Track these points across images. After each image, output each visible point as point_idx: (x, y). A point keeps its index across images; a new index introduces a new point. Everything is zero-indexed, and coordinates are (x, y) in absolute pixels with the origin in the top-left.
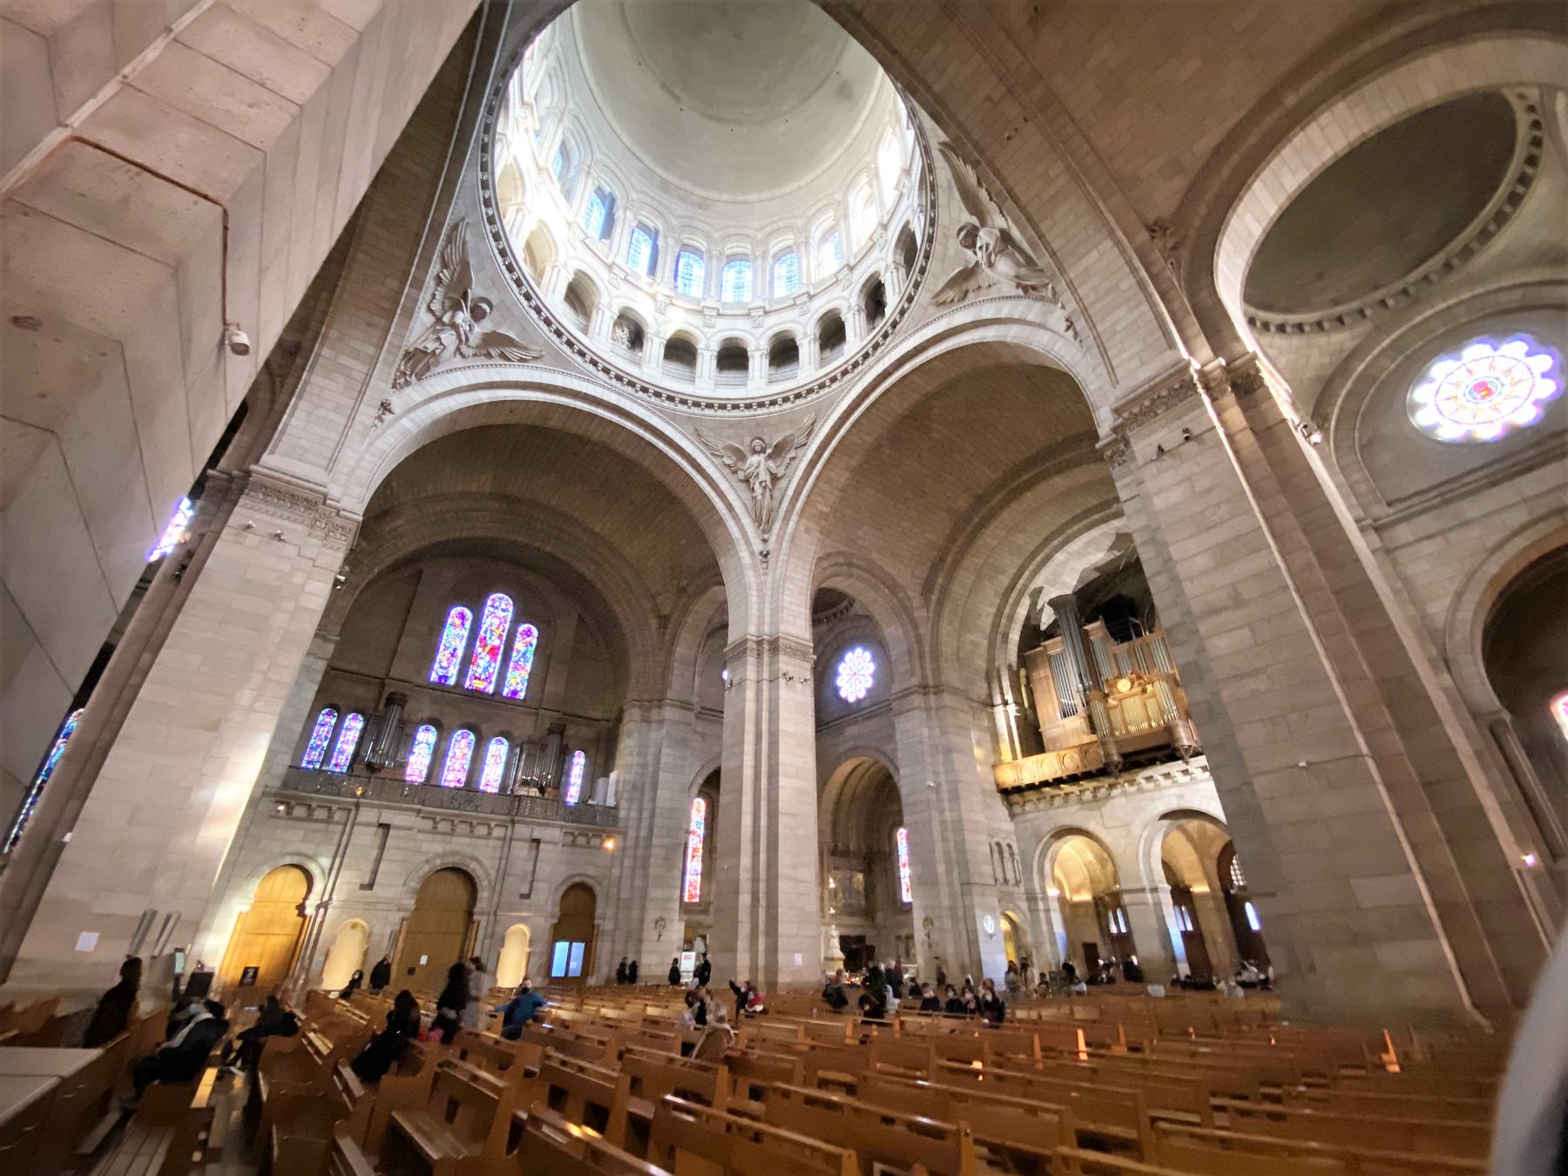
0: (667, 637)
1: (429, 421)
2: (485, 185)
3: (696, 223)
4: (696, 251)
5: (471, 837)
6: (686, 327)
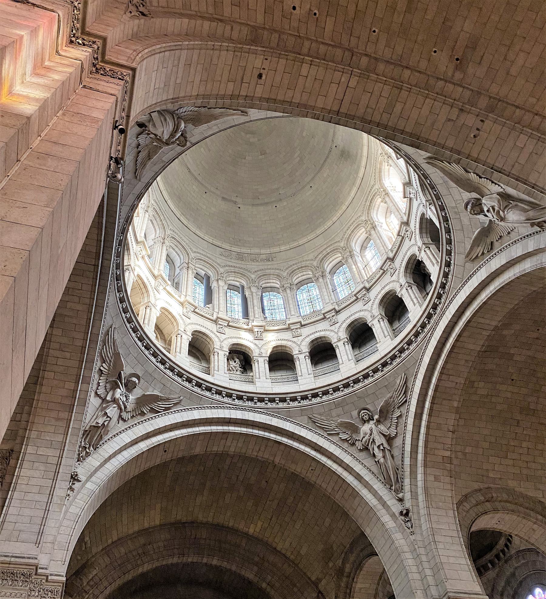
1: (105, 479)
2: (122, 300)
4: (273, 289)
6: (279, 343)
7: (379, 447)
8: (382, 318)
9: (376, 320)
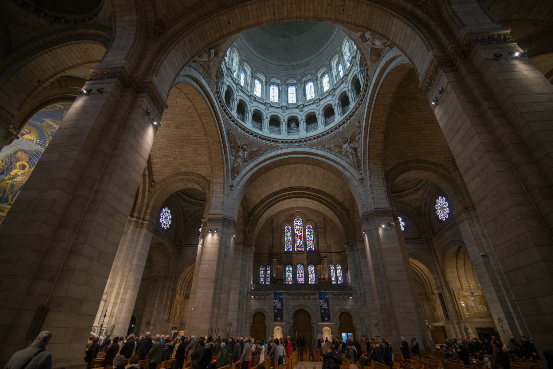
0: (351, 217)
3: (306, 73)
5: (304, 299)
7: (350, 153)
8: (352, 91)
9: (350, 92)
